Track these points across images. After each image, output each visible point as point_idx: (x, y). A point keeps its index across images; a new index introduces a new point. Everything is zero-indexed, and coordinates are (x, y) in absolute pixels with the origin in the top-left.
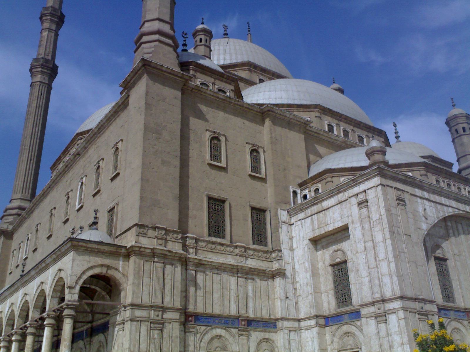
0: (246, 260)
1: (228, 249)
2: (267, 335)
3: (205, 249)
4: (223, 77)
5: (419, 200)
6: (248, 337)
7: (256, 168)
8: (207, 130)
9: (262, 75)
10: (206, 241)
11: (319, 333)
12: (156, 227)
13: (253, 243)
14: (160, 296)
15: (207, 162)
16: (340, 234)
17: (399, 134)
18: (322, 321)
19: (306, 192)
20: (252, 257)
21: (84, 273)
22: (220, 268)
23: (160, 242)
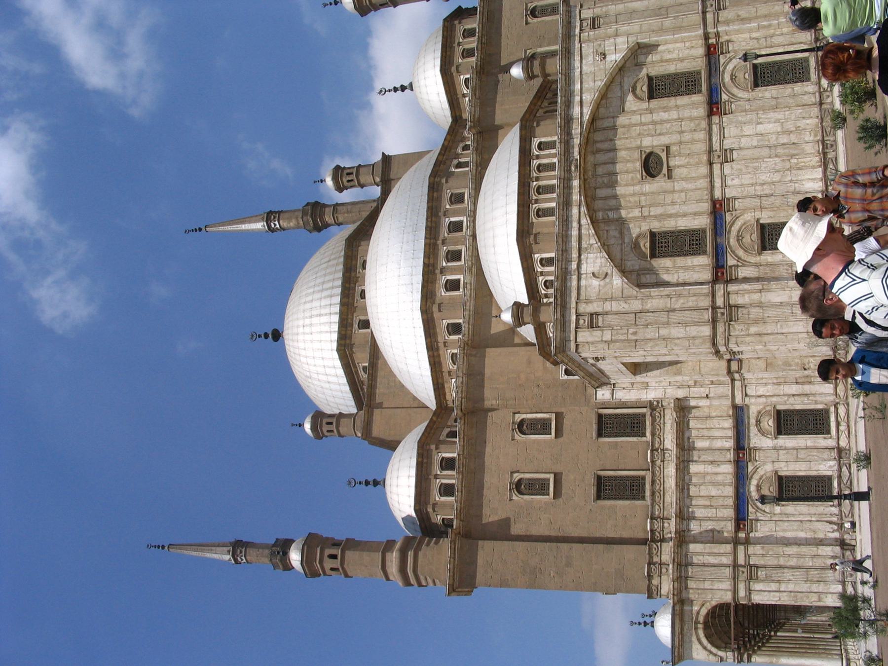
0: (667, 449)
2: (753, 421)
3: (661, 505)
4: (422, 462)
5: (583, 283)
6: (755, 449)
8: (511, 500)
10: (652, 505)
11: (749, 371)
12: (649, 575)
13: (644, 435)
14: (723, 569)
15: (552, 500)
17: (398, 86)
20: (662, 442)
21: (705, 648)
22: (683, 485)
23: (664, 570)
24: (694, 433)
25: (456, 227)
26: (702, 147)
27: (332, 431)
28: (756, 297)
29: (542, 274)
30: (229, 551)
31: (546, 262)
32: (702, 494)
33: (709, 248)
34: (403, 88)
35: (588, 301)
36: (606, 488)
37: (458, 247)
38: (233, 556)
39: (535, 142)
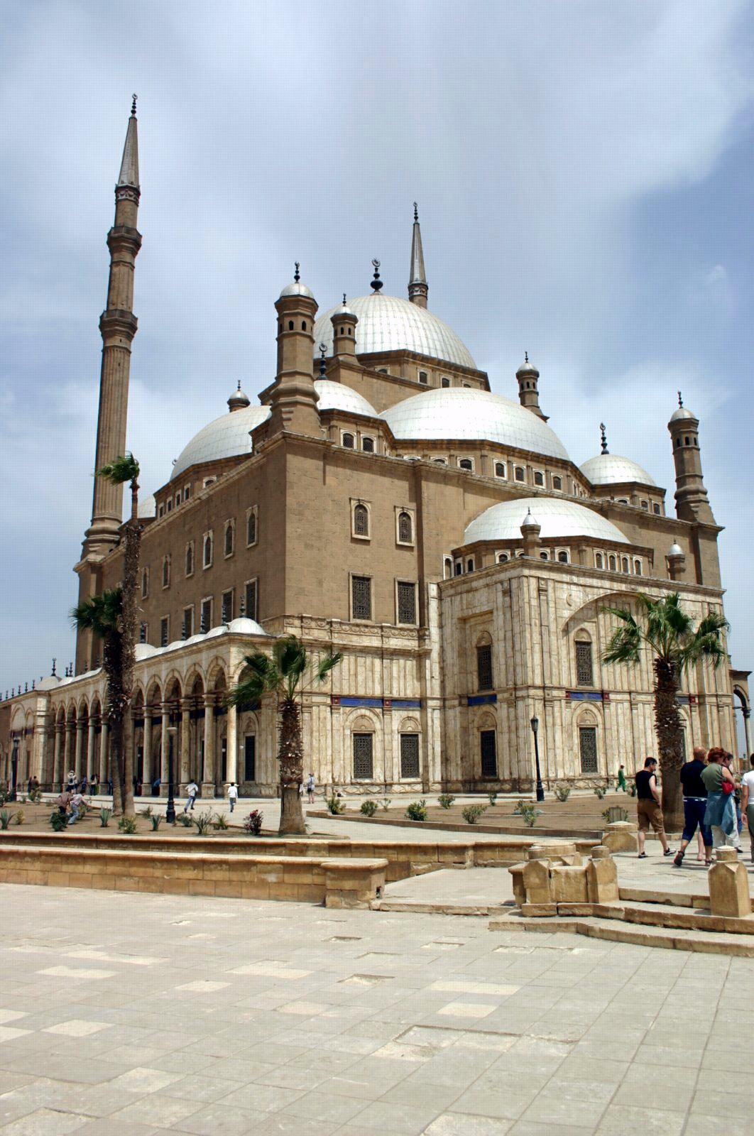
1: (372, 630)
2: (411, 714)
5: (565, 586)
7: (405, 536)
9: (423, 365)
11: (460, 713)
16: (487, 616)
17: (607, 441)
18: (465, 701)
19: (460, 560)
24: (402, 661)
25: (539, 480)
26: (639, 689)
27: (342, 333)
28: (558, 721)
29: (553, 553)
30: (132, 183)
31: (563, 557)
32: (359, 668)
33: (581, 687)
34: (604, 445)
35: (554, 588)
36: (361, 583)
37: (525, 479)
38: (127, 187)
39: (640, 558)
